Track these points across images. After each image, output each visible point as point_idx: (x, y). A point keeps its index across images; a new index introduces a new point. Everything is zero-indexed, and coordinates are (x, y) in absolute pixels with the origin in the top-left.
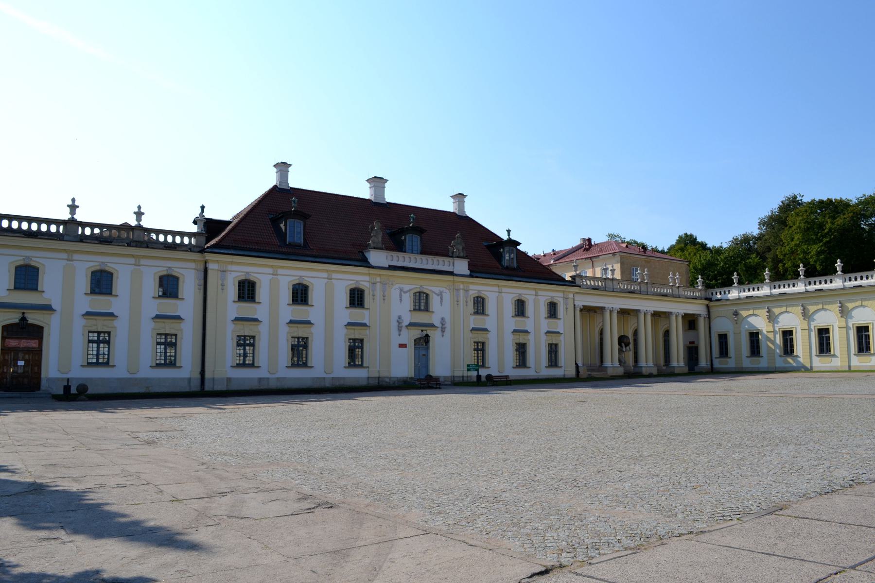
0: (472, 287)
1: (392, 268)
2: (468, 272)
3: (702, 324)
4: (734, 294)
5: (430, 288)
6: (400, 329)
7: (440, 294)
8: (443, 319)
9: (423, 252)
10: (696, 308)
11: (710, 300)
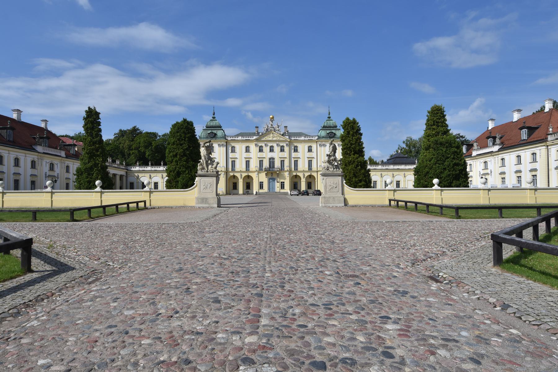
0: (66, 162)
1: (44, 153)
2: (65, 156)
3: (124, 178)
4: (137, 168)
5: (54, 162)
6: (46, 177)
7: (57, 164)
8: (58, 174)
9: (49, 147)
10: (123, 173)
11: (127, 170)
